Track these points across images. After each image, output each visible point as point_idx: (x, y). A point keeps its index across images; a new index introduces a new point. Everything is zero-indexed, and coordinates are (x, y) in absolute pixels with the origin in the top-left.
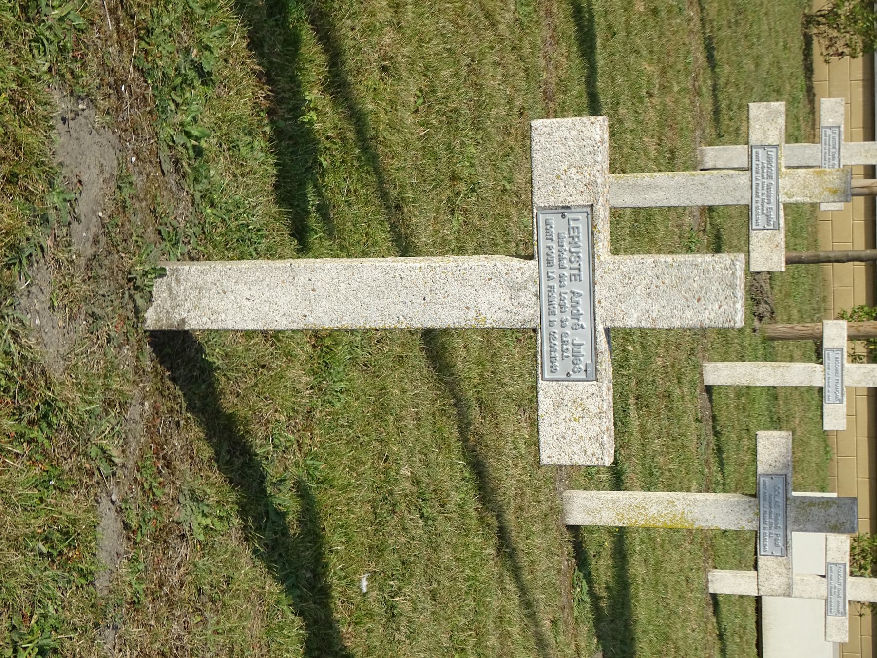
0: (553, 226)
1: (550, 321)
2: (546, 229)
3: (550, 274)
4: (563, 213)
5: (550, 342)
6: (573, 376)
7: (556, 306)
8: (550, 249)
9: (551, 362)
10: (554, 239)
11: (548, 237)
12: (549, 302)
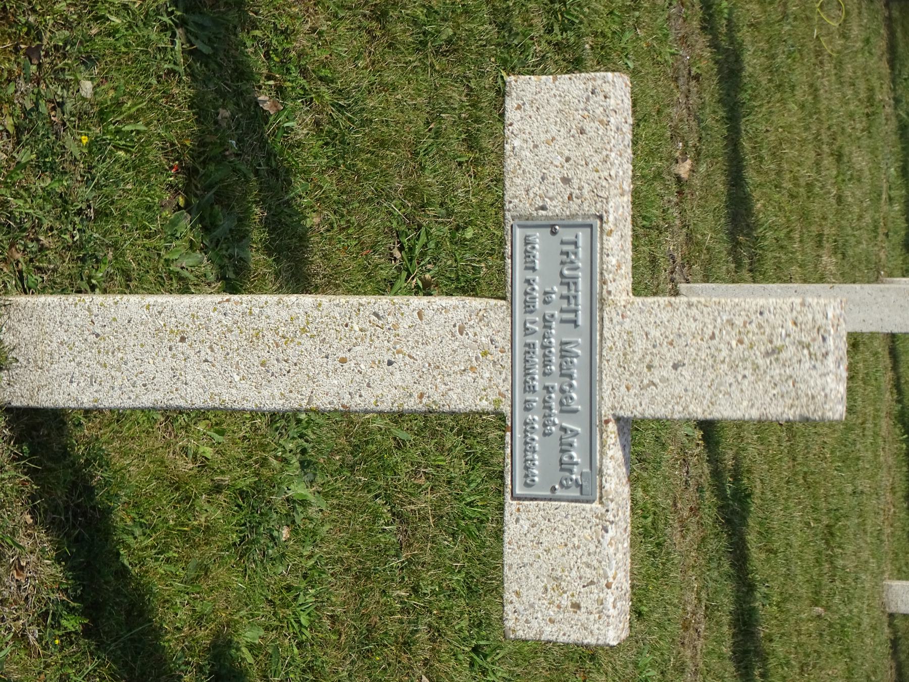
0: (537, 246)
1: (526, 401)
2: (526, 251)
3: (528, 325)
4: (553, 226)
5: (526, 436)
6: (560, 493)
7: (537, 377)
8: (530, 284)
9: (527, 468)
10: (537, 267)
11: (528, 265)
12: (526, 369)
